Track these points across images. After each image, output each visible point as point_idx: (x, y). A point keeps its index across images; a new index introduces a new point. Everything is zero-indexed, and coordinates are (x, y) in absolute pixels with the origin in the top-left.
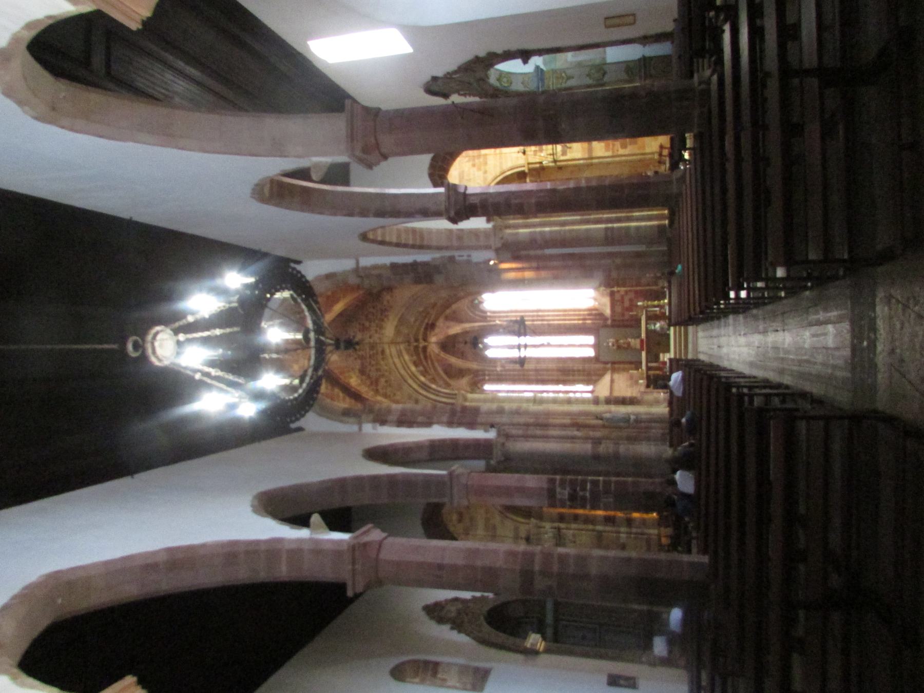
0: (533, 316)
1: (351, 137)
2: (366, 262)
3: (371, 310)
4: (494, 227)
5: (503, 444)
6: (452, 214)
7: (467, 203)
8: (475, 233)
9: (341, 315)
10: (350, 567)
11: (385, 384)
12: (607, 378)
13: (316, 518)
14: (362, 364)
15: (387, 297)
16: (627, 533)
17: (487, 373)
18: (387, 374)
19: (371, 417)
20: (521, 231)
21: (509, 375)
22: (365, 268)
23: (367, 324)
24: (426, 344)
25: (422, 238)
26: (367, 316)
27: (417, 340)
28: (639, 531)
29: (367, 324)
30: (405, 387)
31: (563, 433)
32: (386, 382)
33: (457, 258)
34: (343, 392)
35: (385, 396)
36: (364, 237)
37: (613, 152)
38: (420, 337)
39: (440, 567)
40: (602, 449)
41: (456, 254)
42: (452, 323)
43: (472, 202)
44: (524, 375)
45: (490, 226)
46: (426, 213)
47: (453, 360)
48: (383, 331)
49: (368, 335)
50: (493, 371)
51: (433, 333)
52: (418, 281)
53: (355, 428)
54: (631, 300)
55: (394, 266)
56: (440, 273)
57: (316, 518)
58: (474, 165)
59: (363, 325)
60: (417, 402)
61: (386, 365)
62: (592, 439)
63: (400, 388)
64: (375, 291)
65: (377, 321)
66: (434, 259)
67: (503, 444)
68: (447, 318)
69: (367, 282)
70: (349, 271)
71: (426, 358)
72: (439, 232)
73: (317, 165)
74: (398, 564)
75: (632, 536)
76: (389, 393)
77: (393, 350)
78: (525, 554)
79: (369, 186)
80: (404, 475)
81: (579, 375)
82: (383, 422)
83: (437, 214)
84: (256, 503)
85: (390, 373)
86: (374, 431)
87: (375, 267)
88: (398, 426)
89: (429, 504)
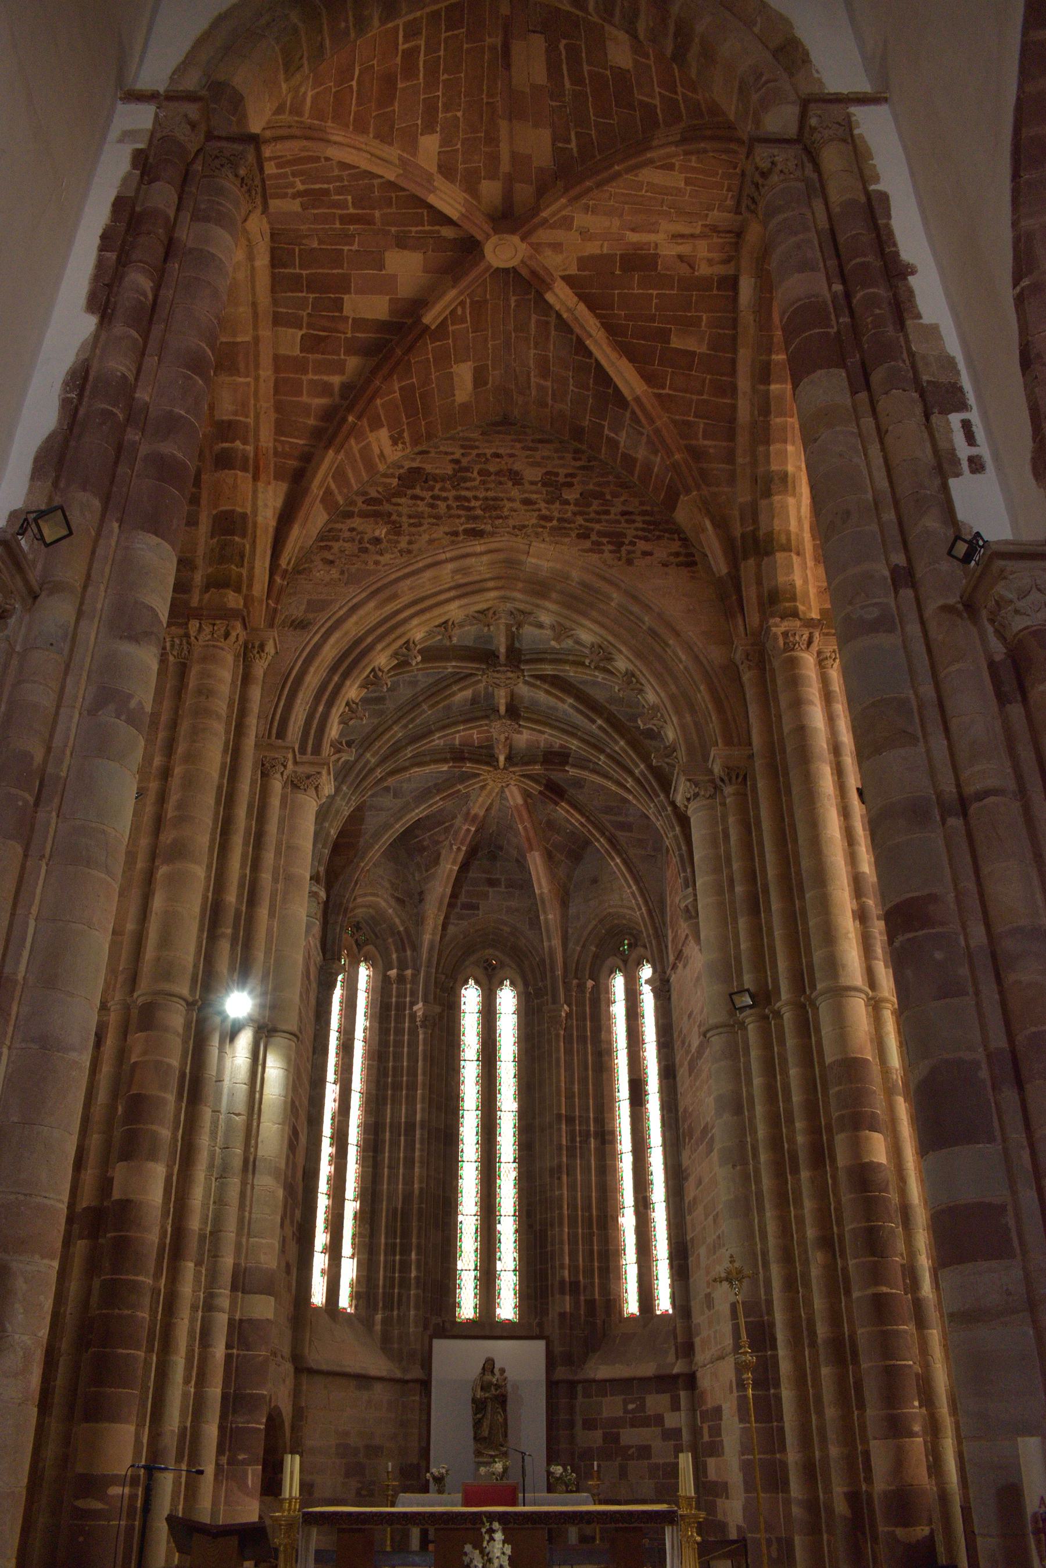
11: (366, 537)
12: (376, 1364)
17: (409, 972)
21: (398, 1044)
22: (848, 124)
26: (599, 496)
29: (571, 495)
32: (377, 541)
33: (955, 419)
35: (327, 537)
44: (397, 1087)
49: (534, 496)
50: (413, 993)
54: (645, 1451)
59: (570, 485)
60: (301, 625)
61: (431, 541)
65: (580, 520)
66: (933, 332)
76: (336, 546)
77: (481, 567)
81: (390, 1267)
86: (114, 133)
88: (119, 204)
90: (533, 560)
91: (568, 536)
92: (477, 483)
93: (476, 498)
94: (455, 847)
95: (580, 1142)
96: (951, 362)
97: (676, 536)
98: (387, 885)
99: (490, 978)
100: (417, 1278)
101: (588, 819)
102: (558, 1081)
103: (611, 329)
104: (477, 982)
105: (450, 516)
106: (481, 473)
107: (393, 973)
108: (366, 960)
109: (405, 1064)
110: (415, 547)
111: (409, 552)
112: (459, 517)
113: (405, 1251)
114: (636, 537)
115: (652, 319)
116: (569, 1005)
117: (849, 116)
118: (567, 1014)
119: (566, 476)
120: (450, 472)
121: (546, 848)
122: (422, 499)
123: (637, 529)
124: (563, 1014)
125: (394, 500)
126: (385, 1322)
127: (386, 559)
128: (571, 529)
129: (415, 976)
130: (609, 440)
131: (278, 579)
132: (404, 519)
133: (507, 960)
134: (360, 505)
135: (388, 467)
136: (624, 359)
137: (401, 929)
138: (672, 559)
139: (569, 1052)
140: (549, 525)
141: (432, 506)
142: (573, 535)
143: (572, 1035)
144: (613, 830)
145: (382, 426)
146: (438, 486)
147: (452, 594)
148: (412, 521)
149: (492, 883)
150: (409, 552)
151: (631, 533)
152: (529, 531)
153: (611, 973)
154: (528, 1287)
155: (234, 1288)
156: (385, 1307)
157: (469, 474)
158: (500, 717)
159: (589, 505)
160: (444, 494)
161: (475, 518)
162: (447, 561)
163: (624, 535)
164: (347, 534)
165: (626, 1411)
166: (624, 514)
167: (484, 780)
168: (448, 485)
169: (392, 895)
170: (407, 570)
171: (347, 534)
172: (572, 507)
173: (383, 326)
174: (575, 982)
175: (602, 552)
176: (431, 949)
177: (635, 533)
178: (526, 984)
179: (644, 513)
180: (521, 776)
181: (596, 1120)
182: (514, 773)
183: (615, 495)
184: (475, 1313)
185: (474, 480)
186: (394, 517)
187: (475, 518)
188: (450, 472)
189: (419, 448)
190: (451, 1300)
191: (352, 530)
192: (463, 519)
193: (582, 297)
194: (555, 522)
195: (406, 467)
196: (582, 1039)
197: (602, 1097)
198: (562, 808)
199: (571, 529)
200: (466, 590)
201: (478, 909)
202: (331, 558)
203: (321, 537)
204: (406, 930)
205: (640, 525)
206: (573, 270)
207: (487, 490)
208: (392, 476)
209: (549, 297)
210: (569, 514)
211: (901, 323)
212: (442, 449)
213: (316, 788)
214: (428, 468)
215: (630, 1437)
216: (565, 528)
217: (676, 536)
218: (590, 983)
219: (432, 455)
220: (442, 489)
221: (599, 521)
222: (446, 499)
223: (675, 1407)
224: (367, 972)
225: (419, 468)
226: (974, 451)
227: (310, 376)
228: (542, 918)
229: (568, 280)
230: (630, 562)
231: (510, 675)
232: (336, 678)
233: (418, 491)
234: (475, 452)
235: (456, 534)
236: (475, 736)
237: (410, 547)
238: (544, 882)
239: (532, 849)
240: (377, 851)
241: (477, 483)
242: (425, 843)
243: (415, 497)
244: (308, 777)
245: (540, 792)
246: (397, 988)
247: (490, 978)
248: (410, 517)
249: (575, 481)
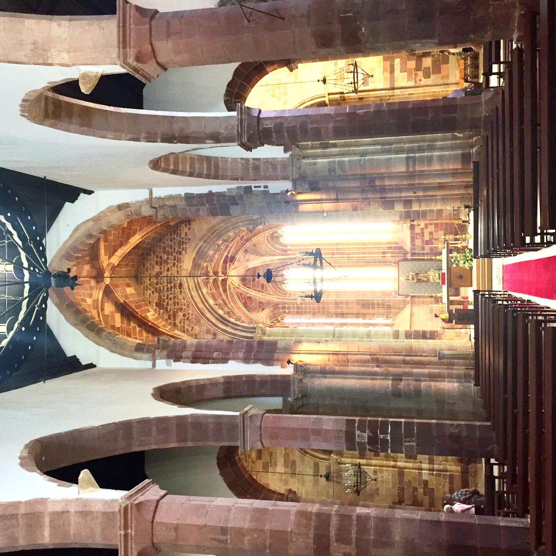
1: (124, 42)
2: (159, 192)
3: (169, 242)
4: (291, 155)
5: (301, 381)
6: (245, 140)
7: (261, 128)
8: (272, 163)
9: (137, 247)
10: (122, 532)
11: (183, 318)
12: (407, 311)
13: (85, 475)
14: (160, 297)
15: (185, 229)
16: (430, 470)
17: (287, 305)
18: (183, 307)
19: (165, 353)
20: (319, 160)
22: (159, 199)
23: (165, 257)
25: (217, 167)
26: (165, 248)
27: (216, 273)
28: (441, 467)
29: (165, 257)
30: (203, 321)
31: (363, 369)
32: (184, 315)
33: (253, 189)
34: (139, 327)
36: (156, 164)
37: (415, 82)
38: (220, 270)
39: (224, 531)
40: (402, 385)
41: (253, 184)
42: (252, 257)
43: (265, 126)
45: (287, 155)
46: (217, 138)
47: (253, 293)
48: (181, 264)
49: (166, 268)
50: (293, 304)
51: (232, 266)
52: (213, 213)
53: (148, 364)
54: (431, 233)
55: (189, 197)
56: (238, 204)
57: (85, 475)
58: (274, 96)
59: (161, 257)
60: (215, 335)
61: (184, 299)
62: (393, 375)
63: (198, 322)
64: (172, 224)
65: (174, 254)
66: (229, 190)
67: (301, 381)
68: (246, 251)
69: (161, 213)
70: (142, 202)
71: (225, 290)
72: (235, 160)
73: (85, 76)
74: (176, 528)
75: (435, 473)
76: (186, 327)
78: (319, 515)
79: (156, 110)
80: (192, 415)
82: (177, 359)
83: (229, 139)
84: (25, 454)
85: (188, 307)
87: (170, 197)
88: (192, 362)
89: (221, 447)
90: (190, 269)
91: (180, 258)
92: (161, 286)
93: (167, 286)
94: (248, 292)
96: (238, 187)
97: (179, 225)
98: (258, 314)
101: (240, 249)
103: (121, 245)
105: (175, 293)
106: (157, 284)
107: (287, 311)
110: (186, 304)
111: (188, 305)
112: (174, 291)
114: (180, 238)
115: (119, 232)
117: (156, 198)
119: (157, 257)
120: (157, 294)
121: (246, 262)
122: (168, 302)
123: (177, 237)
125: (169, 310)
126: (394, 308)
127: (191, 312)
128: (178, 257)
130: (147, 244)
132: (176, 307)
134: (171, 321)
135: (156, 313)
136: (129, 241)
137: (272, 308)
138: (188, 226)
140: (176, 264)
141: (171, 299)
142: (180, 256)
144: (243, 241)
145: (146, 315)
146: (163, 297)
147: (200, 292)
148: (176, 305)
150: (188, 305)
151: (178, 239)
152: (179, 269)
155: (398, 338)
156: (390, 309)
157: (158, 288)
159: (168, 251)
160: (166, 296)
161: (175, 286)
162: (191, 294)
163: (179, 241)
164: (182, 324)
165: (420, 238)
166: (171, 241)
168: (162, 294)
170: (195, 306)
171: (182, 324)
172: (170, 257)
173: (122, 314)
174: (288, 252)
175: (186, 248)
177: (178, 238)
179: (171, 235)
183: (164, 243)
185: (160, 286)
186: (175, 310)
187: (175, 286)
188: (157, 294)
189: (149, 305)
191: (180, 323)
192: (176, 289)
193: (113, 254)
194: (176, 262)
195: (156, 307)
199: (178, 257)
200: (198, 287)
202: (191, 329)
203: (184, 332)
204: (272, 307)
205: (175, 236)
206: (107, 257)
207: (164, 282)
208: (159, 312)
209: (116, 264)
210: (172, 257)
211: (226, 196)
212: (148, 297)
214: (155, 301)
215: (427, 237)
216: (178, 259)
217: (179, 225)
218: (289, 247)
219: (151, 300)
220: (164, 296)
221: (175, 248)
222: (168, 295)
223: (419, 225)
225: (156, 303)
226: (262, 187)
227: (138, 336)
229: (109, 258)
230: (189, 239)
232: (230, 324)
233: (165, 304)
234: (149, 287)
235: (181, 292)
237: (186, 305)
239: (247, 267)
241: (161, 286)
243: (168, 304)
244: (262, 330)
248: (175, 305)
249: (159, 255)
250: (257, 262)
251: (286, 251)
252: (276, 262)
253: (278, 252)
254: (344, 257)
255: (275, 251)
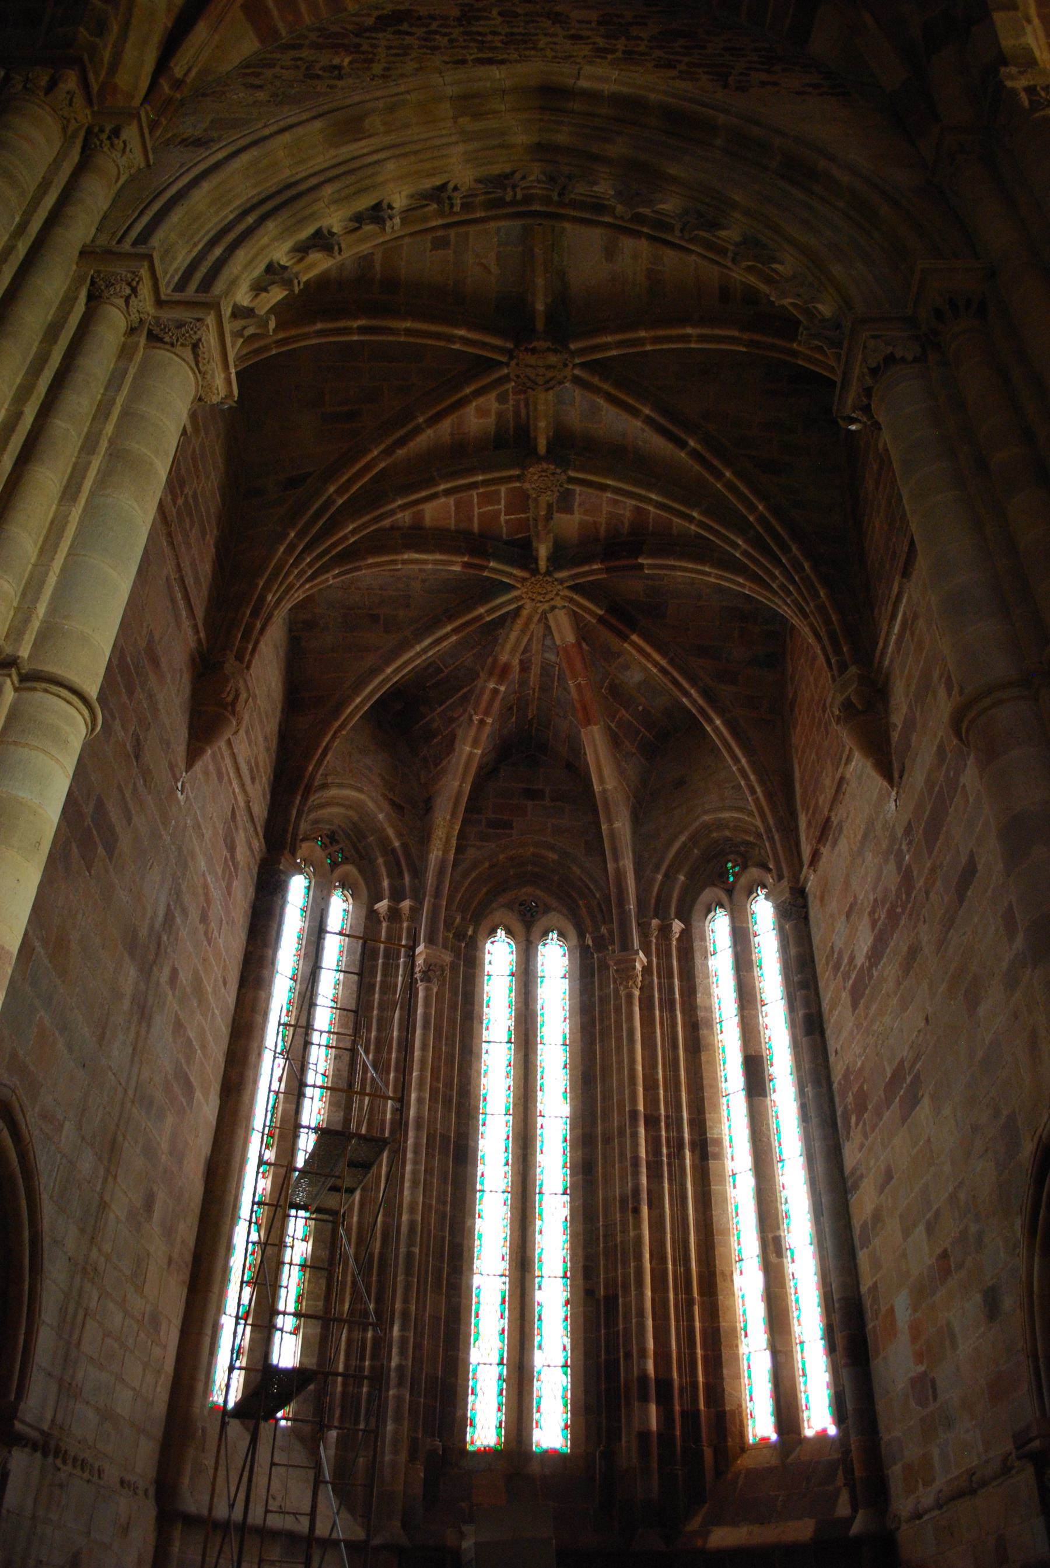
0: (675, 1123)
17: (406, 904)
24: (543, 564)
94: (476, 718)
95: (669, 1156)
99: (528, 925)
100: (400, 1368)
102: (632, 1061)
104: (509, 932)
107: (382, 906)
108: (343, 886)
109: (395, 1034)
113: (383, 1319)
116: (648, 954)
118: (644, 967)
124: (638, 967)
129: (415, 911)
131: (165, 87)
133: (555, 904)
139: (648, 1021)
143: (651, 998)
149: (534, 795)
153: (709, 911)
154: (586, 1392)
158: (540, 459)
167: (517, 598)
169: (384, 796)
174: (655, 922)
176: (441, 873)
178: (581, 936)
180: (571, 588)
181: (691, 1122)
182: (561, 582)
184: (499, 1436)
190: (459, 1413)
196: (668, 1004)
197: (701, 1088)
198: (633, 644)
201: (512, 828)
204: (405, 846)
213: (195, 347)
218: (677, 926)
224: (345, 906)
228: (604, 827)
231: (553, 359)
236: (503, 518)
238: (607, 771)
239: (588, 722)
240: (358, 708)
242: (435, 725)
244: (180, 325)
245: (601, 620)
246: (388, 928)
247: (528, 925)
250: (607, 771)
251: (661, 910)
252: (610, 866)
253: (652, 880)
254: (636, 1174)
255: (657, 869)
